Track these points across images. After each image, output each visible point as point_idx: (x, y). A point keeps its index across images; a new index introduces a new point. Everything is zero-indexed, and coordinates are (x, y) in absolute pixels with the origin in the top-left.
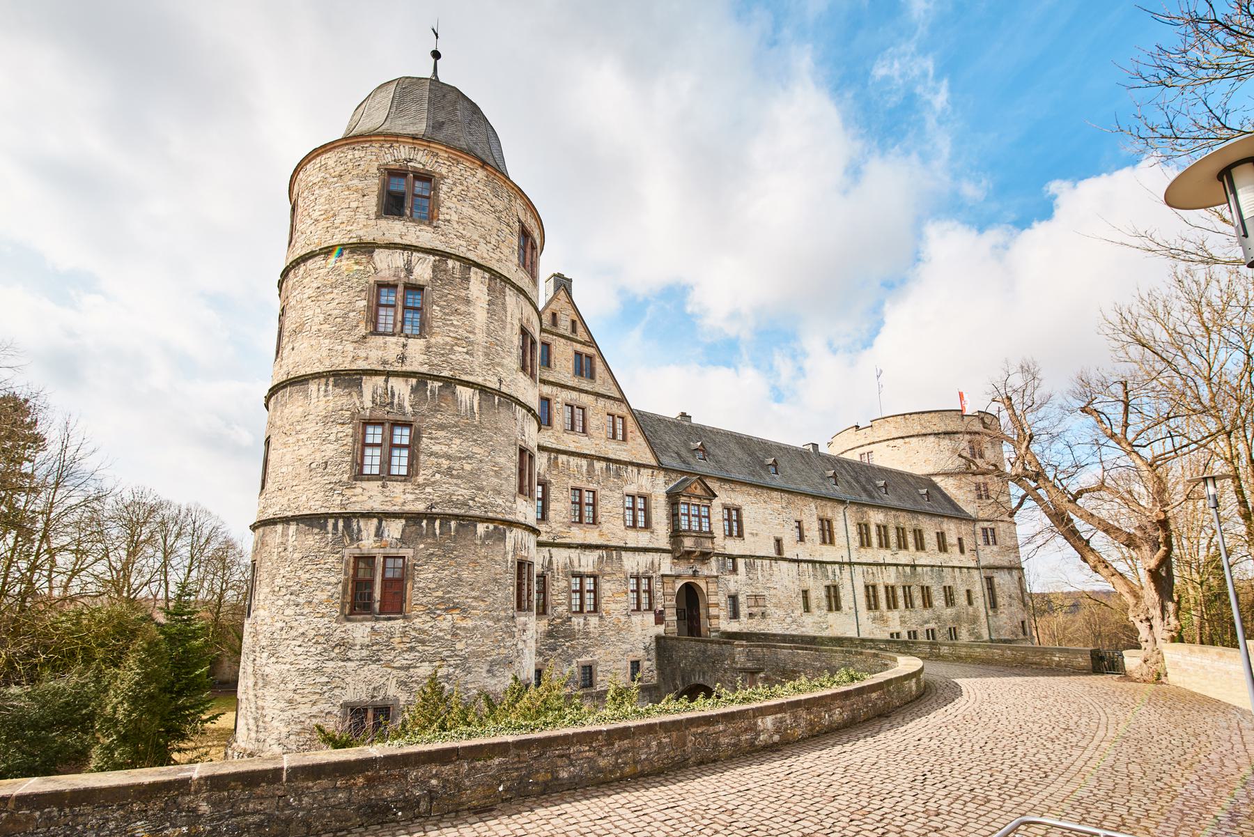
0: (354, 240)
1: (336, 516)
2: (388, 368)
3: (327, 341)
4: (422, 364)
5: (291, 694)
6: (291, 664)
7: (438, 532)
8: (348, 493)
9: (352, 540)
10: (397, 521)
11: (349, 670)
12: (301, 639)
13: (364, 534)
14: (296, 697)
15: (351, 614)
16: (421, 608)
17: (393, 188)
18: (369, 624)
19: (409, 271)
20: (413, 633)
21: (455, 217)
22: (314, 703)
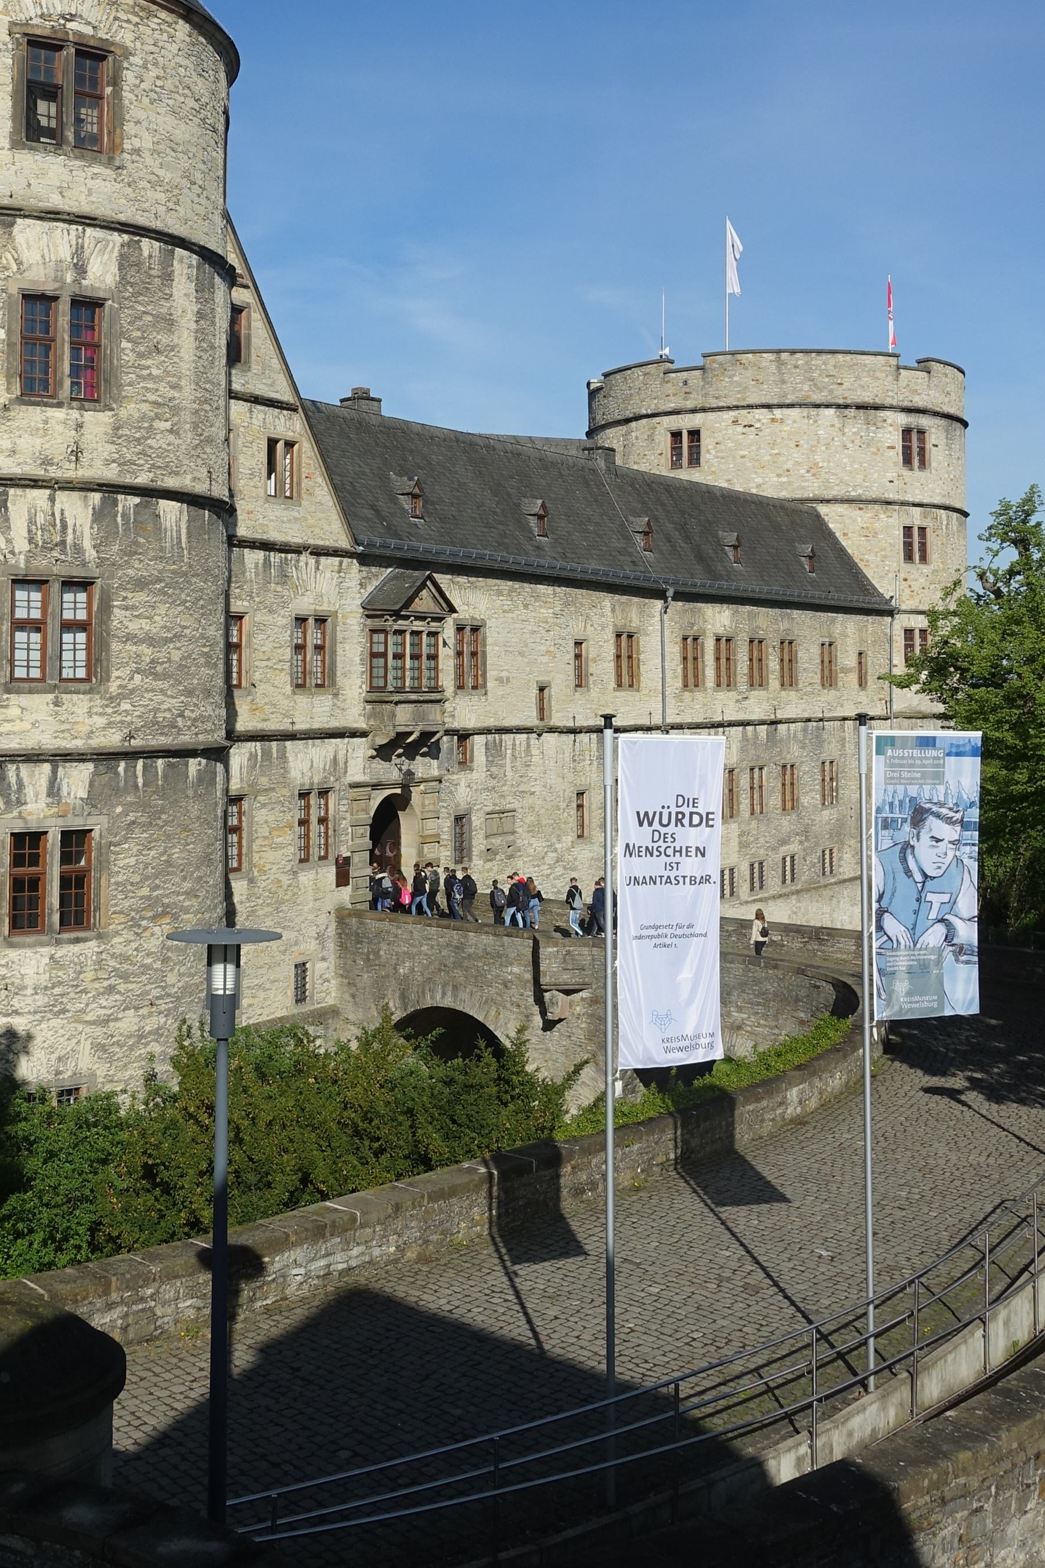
4: (107, 462)
10: (82, 766)
16: (122, 919)
18: (45, 950)
20: (112, 963)
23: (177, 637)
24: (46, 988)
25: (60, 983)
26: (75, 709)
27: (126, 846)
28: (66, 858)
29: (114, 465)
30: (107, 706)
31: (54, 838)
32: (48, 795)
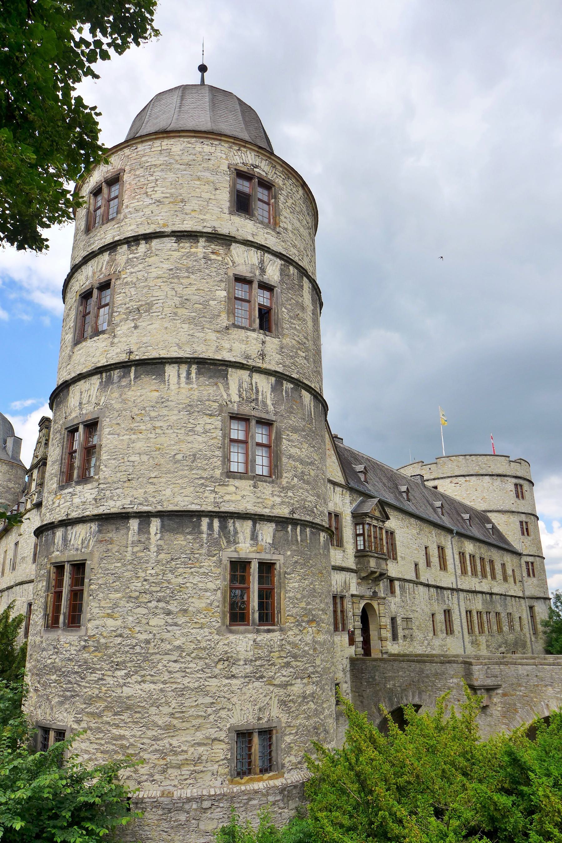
0: (209, 230)
1: (211, 515)
2: (251, 363)
3: (186, 326)
4: (278, 364)
5: (167, 719)
6: (164, 682)
7: (299, 538)
8: (221, 490)
9: (228, 542)
10: (269, 524)
11: (235, 688)
12: (176, 654)
13: (241, 536)
14: (175, 722)
15: (231, 625)
16: (292, 620)
17: (239, 187)
18: (250, 636)
19: (263, 271)
20: (288, 647)
21: (290, 227)
22: (198, 728)
23: (312, 463)
24: (251, 660)
25: (260, 658)
26: (264, 491)
27: (293, 575)
28: (261, 580)
29: (281, 366)
30: (281, 492)
31: (255, 565)
32: (252, 539)
